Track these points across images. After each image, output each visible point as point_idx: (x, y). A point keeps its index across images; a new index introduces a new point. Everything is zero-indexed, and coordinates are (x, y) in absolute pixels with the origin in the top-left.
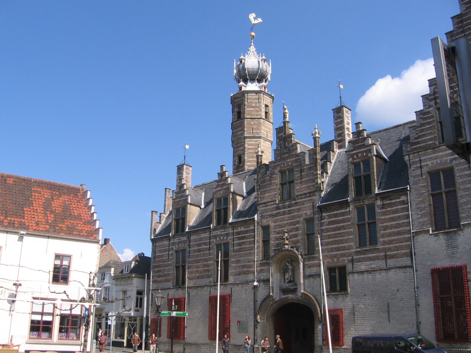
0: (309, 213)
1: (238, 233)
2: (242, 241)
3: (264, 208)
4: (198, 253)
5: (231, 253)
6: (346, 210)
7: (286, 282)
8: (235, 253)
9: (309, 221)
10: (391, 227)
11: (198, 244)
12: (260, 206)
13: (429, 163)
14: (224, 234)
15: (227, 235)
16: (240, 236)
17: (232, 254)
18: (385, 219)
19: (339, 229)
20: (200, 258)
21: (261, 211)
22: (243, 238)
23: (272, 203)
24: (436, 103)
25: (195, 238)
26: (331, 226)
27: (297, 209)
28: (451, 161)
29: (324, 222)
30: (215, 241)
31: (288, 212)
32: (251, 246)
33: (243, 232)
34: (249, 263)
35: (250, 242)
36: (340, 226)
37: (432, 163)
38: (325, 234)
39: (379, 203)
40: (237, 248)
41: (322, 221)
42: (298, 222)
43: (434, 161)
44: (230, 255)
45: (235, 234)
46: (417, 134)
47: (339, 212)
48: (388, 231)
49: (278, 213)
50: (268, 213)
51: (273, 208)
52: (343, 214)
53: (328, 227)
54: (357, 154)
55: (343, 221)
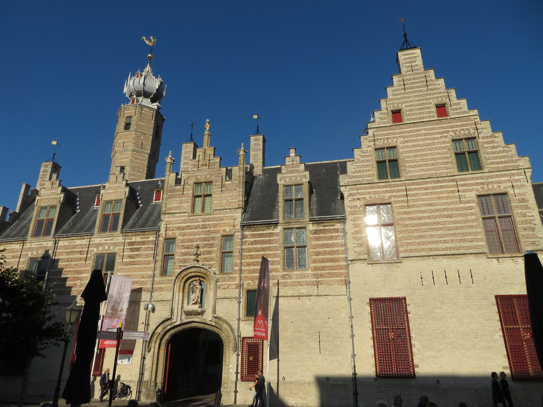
0: (228, 230)
1: (131, 244)
6: (273, 232)
7: (191, 303)
10: (325, 253)
12: (166, 216)
13: (367, 197)
16: (133, 247)
17: (120, 267)
18: (318, 245)
20: (68, 269)
22: (138, 250)
24: (375, 144)
26: (254, 246)
27: (214, 224)
29: (246, 241)
30: (95, 250)
32: (147, 259)
33: (139, 243)
36: (266, 248)
37: (370, 197)
38: (248, 254)
39: (311, 227)
40: (128, 260)
41: (244, 240)
43: (373, 196)
44: (116, 268)
45: (126, 245)
46: (355, 168)
48: (321, 257)
50: (175, 225)
52: (270, 235)
53: (250, 246)
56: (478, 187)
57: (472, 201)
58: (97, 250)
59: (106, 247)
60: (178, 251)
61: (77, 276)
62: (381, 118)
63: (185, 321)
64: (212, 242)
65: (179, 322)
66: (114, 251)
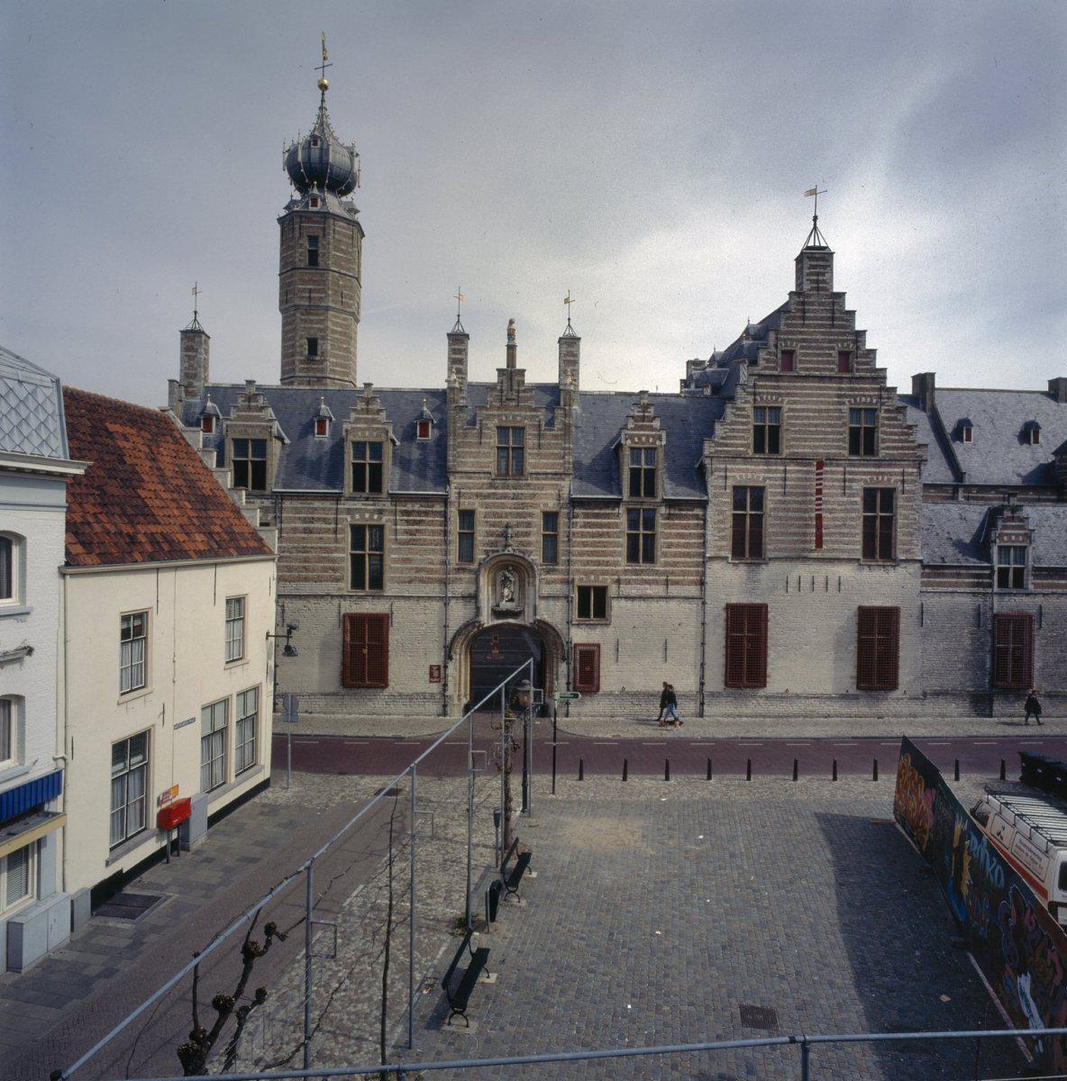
1: (407, 513)
2: (416, 527)
4: (303, 535)
5: (388, 545)
9: (550, 518)
14: (374, 510)
15: (380, 512)
16: (411, 518)
19: (601, 535)
24: (755, 400)
26: (589, 530)
28: (765, 479)
30: (349, 519)
33: (419, 513)
35: (433, 531)
38: (579, 539)
39: (663, 510)
40: (405, 537)
42: (531, 515)
47: (602, 511)
53: (582, 530)
54: (640, 437)
55: (608, 526)
56: (868, 477)
57: (858, 494)
58: (352, 518)
59: (367, 516)
60: (481, 531)
62: (767, 361)
64: (529, 519)
66: (380, 523)
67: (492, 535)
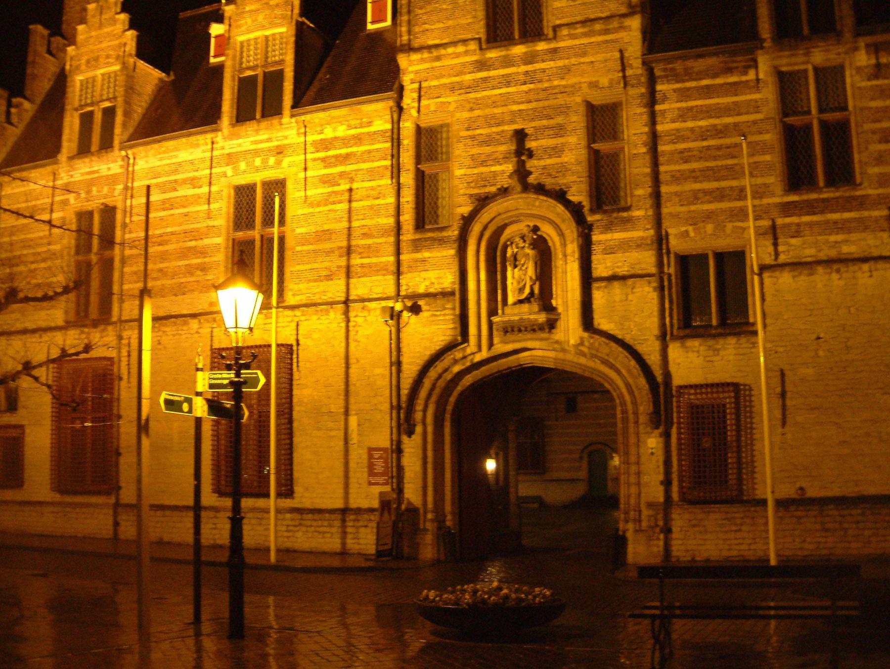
1: (325, 145)
3: (427, 66)
8: (311, 210)
11: (164, 183)
12: (415, 57)
15: (280, 151)
16: (332, 153)
17: (300, 212)
21: (416, 72)
22: (345, 159)
23: (461, 49)
25: (151, 165)
31: (522, 77)
34: (369, 241)
35: (370, 171)
45: (310, 149)
49: (485, 80)
51: (464, 65)
58: (236, 169)
61: (193, 243)
63: (500, 347)
64: (559, 120)
65: (484, 354)
67: (483, 163)
